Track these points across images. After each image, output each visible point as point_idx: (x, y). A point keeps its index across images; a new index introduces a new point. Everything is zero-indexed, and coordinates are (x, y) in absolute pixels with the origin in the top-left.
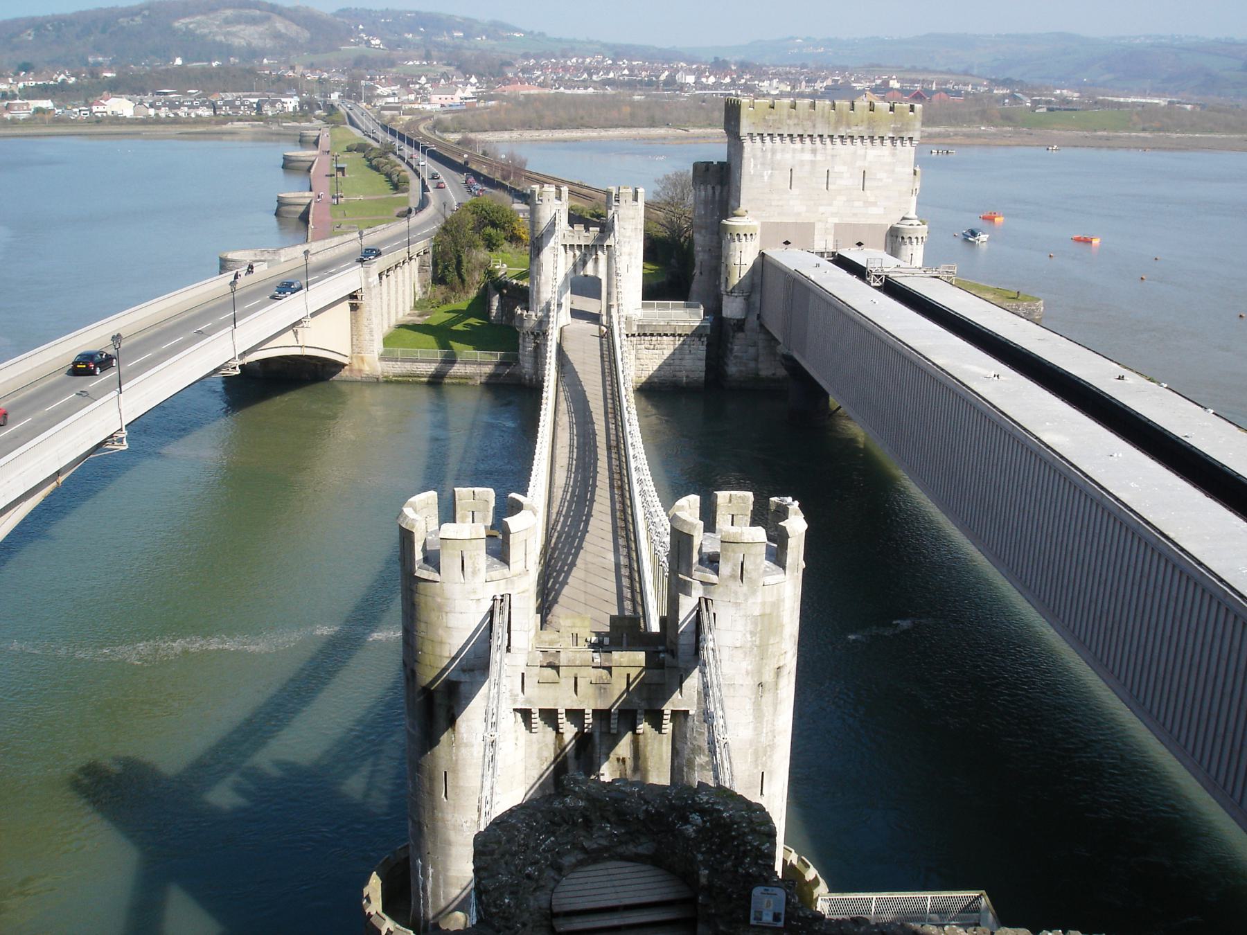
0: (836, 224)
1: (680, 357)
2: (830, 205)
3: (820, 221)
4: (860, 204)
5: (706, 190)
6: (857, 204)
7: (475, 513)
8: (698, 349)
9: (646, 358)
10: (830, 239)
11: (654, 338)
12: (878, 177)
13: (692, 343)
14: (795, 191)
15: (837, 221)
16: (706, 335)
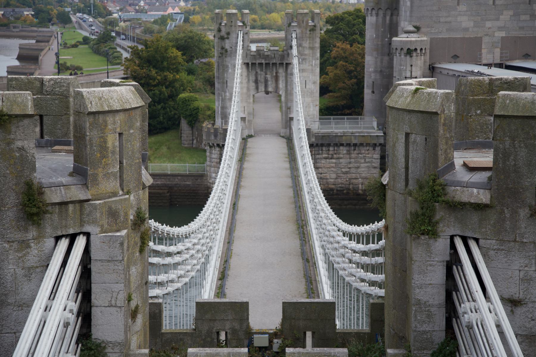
0: (502, 37)
1: (356, 165)
2: (498, 19)
3: (487, 35)
4: (527, 17)
5: (377, 15)
7: (45, 118)
8: (372, 158)
9: (324, 167)
10: (498, 51)
11: (331, 149)
13: (367, 152)
14: (462, 8)
15: (503, 34)
16: (380, 144)
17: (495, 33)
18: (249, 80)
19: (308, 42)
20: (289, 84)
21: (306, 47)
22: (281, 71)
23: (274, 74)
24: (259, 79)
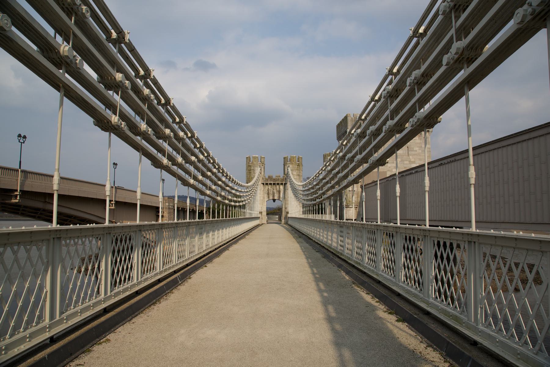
3: (389, 171)
4: (408, 162)
6: (405, 162)
12: (414, 150)
17: (393, 170)
18: (264, 193)
19: (296, 172)
20: (286, 195)
21: (295, 175)
22: (282, 187)
23: (278, 190)
24: (270, 192)
